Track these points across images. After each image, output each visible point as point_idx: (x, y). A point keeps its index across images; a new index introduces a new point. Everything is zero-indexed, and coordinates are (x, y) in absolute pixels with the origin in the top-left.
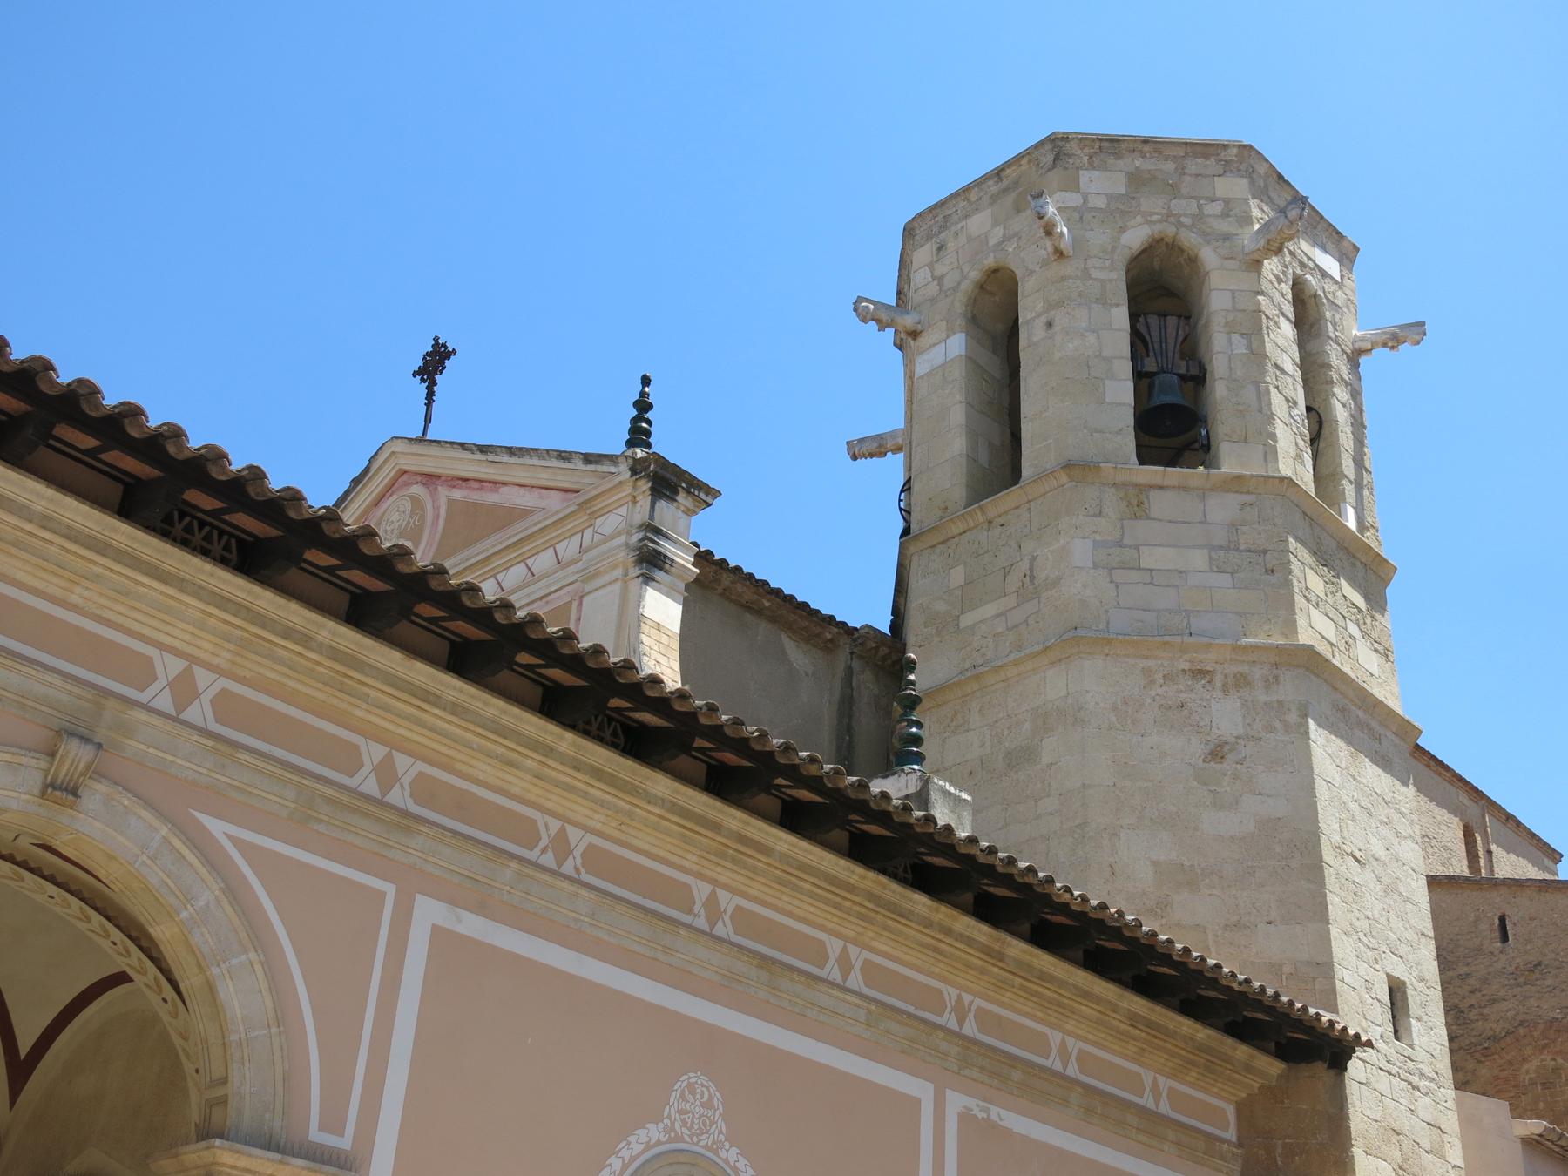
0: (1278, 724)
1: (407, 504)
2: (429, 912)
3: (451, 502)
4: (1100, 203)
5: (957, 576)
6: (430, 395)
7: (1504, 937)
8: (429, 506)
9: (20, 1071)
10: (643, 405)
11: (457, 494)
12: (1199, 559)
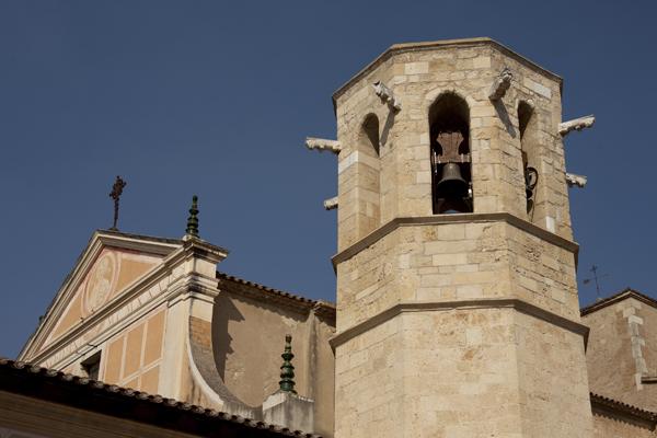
0: (499, 338)
3: (123, 260)
4: (413, 79)
5: (355, 275)
6: (117, 205)
8: (114, 260)
10: (194, 212)
11: (125, 256)
12: (462, 259)
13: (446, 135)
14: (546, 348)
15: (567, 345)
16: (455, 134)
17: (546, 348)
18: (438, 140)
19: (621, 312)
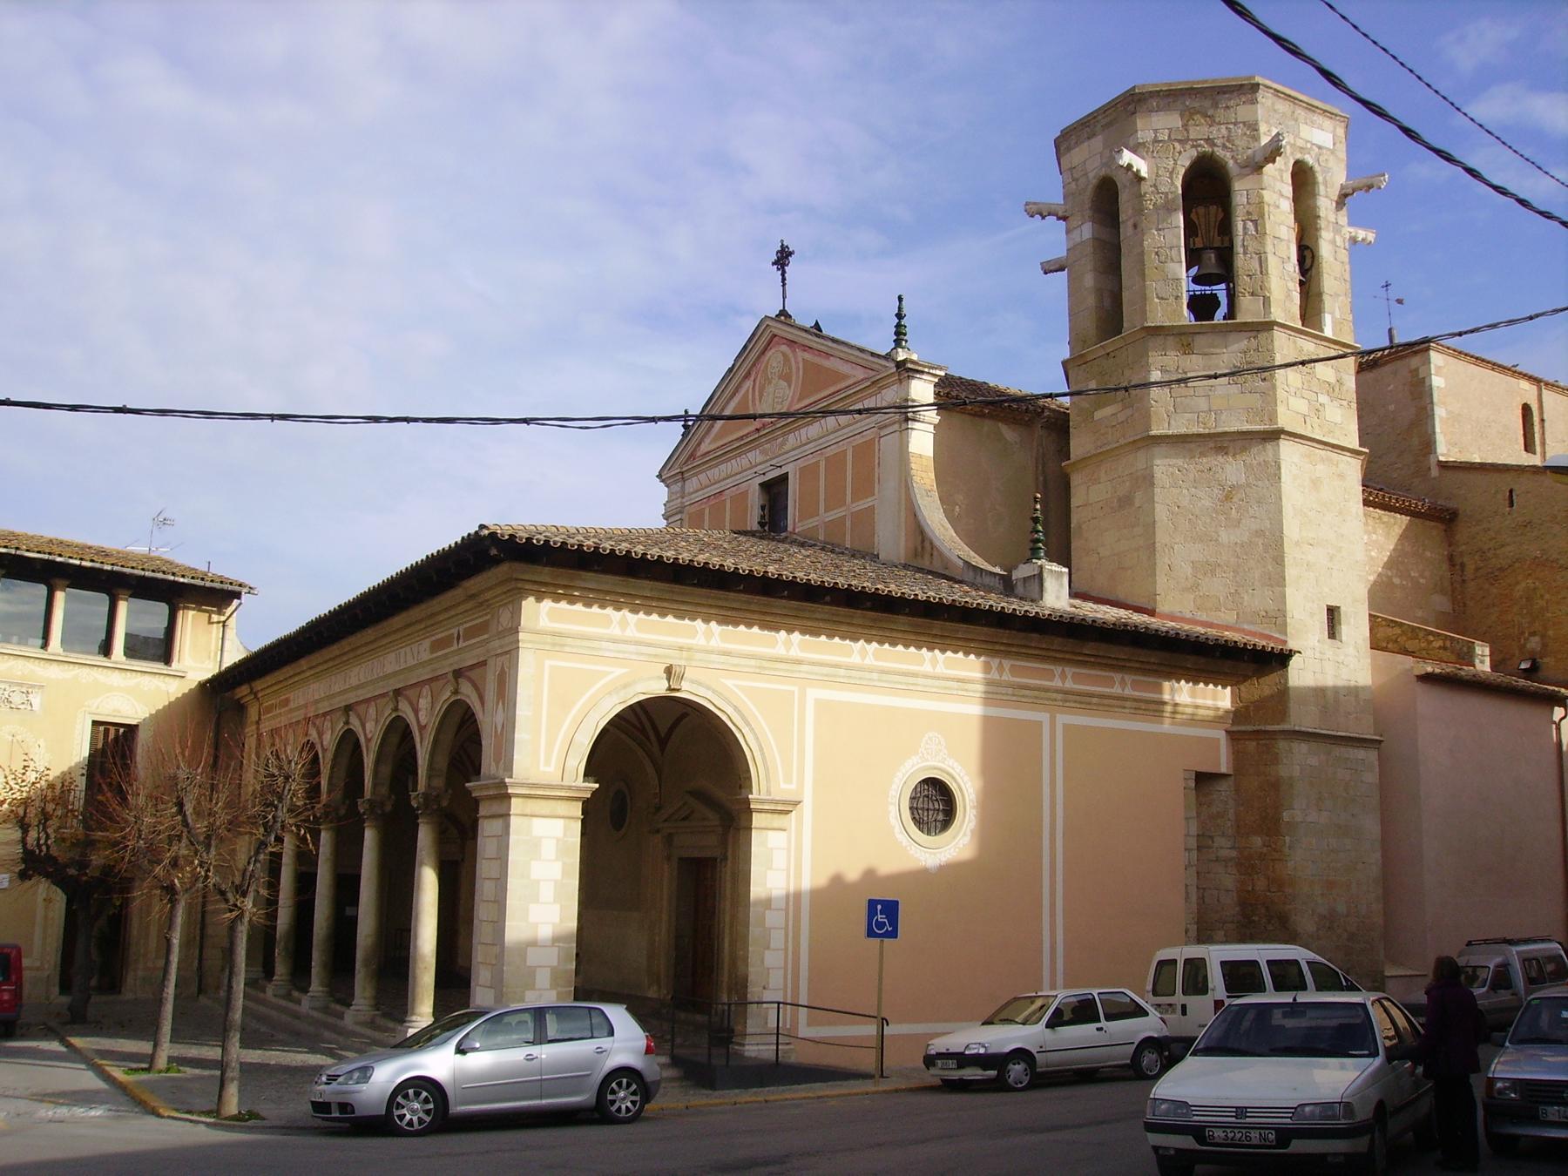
1: (780, 357)
2: (813, 693)
6: (784, 279)
7: (1511, 504)
9: (663, 742)
11: (807, 356)
13: (1201, 210)
14: (1316, 483)
15: (1341, 476)
16: (1213, 209)
17: (1316, 483)
18: (1193, 216)
19: (1417, 370)
